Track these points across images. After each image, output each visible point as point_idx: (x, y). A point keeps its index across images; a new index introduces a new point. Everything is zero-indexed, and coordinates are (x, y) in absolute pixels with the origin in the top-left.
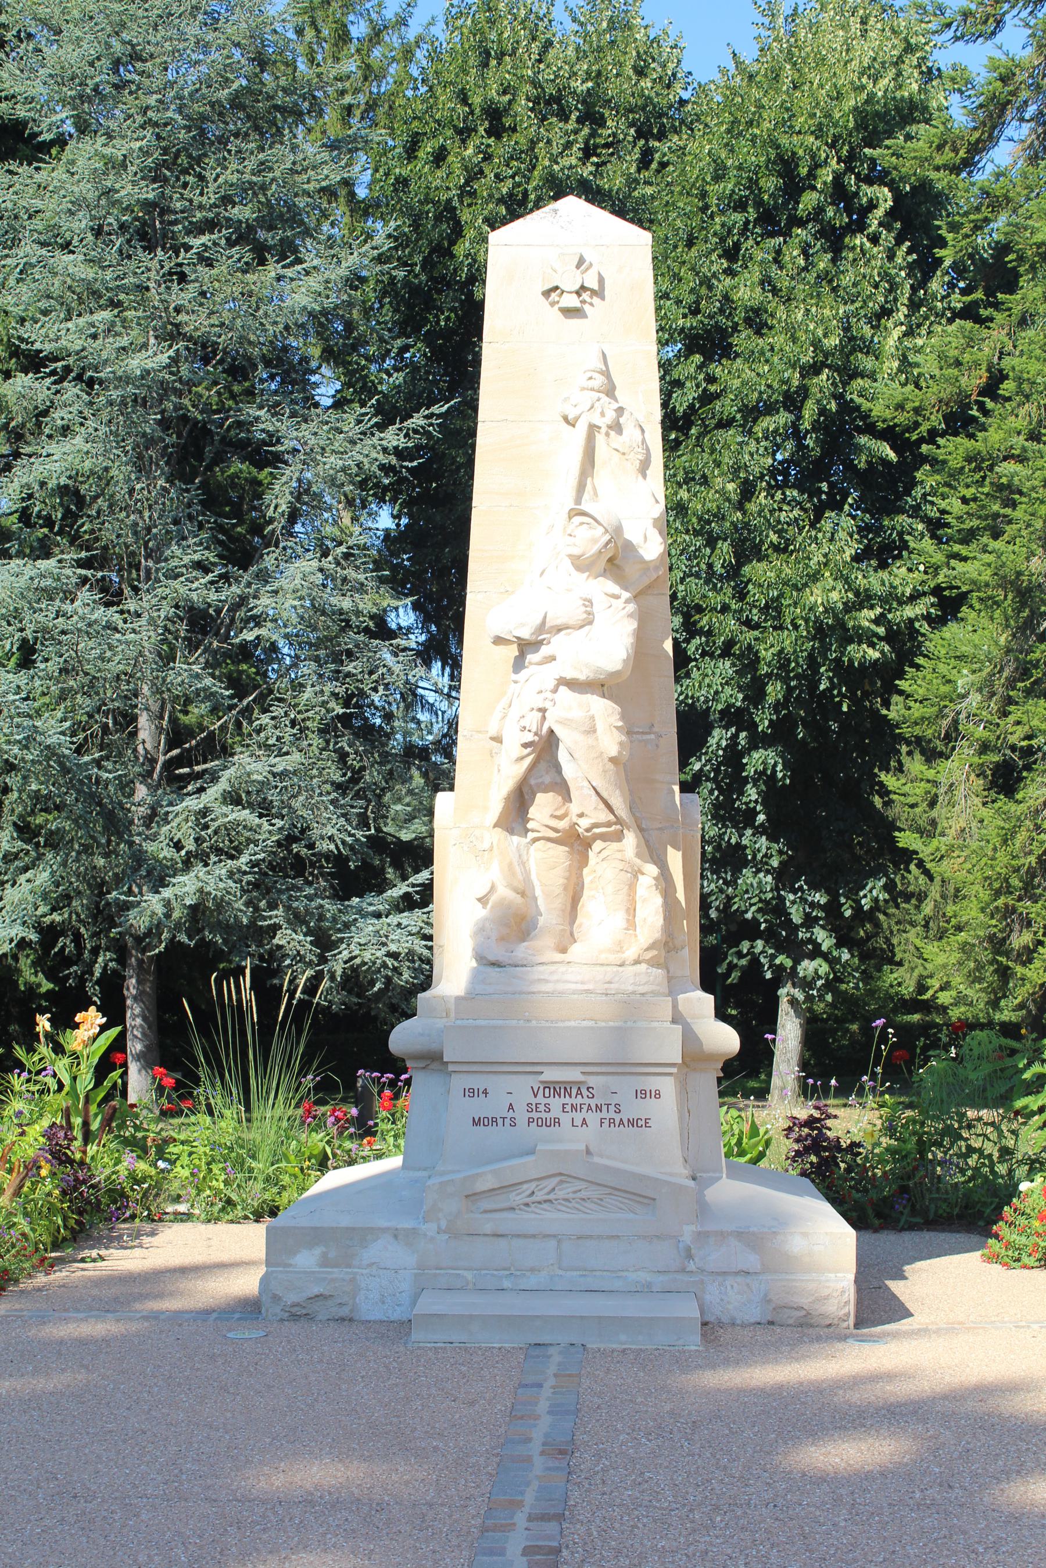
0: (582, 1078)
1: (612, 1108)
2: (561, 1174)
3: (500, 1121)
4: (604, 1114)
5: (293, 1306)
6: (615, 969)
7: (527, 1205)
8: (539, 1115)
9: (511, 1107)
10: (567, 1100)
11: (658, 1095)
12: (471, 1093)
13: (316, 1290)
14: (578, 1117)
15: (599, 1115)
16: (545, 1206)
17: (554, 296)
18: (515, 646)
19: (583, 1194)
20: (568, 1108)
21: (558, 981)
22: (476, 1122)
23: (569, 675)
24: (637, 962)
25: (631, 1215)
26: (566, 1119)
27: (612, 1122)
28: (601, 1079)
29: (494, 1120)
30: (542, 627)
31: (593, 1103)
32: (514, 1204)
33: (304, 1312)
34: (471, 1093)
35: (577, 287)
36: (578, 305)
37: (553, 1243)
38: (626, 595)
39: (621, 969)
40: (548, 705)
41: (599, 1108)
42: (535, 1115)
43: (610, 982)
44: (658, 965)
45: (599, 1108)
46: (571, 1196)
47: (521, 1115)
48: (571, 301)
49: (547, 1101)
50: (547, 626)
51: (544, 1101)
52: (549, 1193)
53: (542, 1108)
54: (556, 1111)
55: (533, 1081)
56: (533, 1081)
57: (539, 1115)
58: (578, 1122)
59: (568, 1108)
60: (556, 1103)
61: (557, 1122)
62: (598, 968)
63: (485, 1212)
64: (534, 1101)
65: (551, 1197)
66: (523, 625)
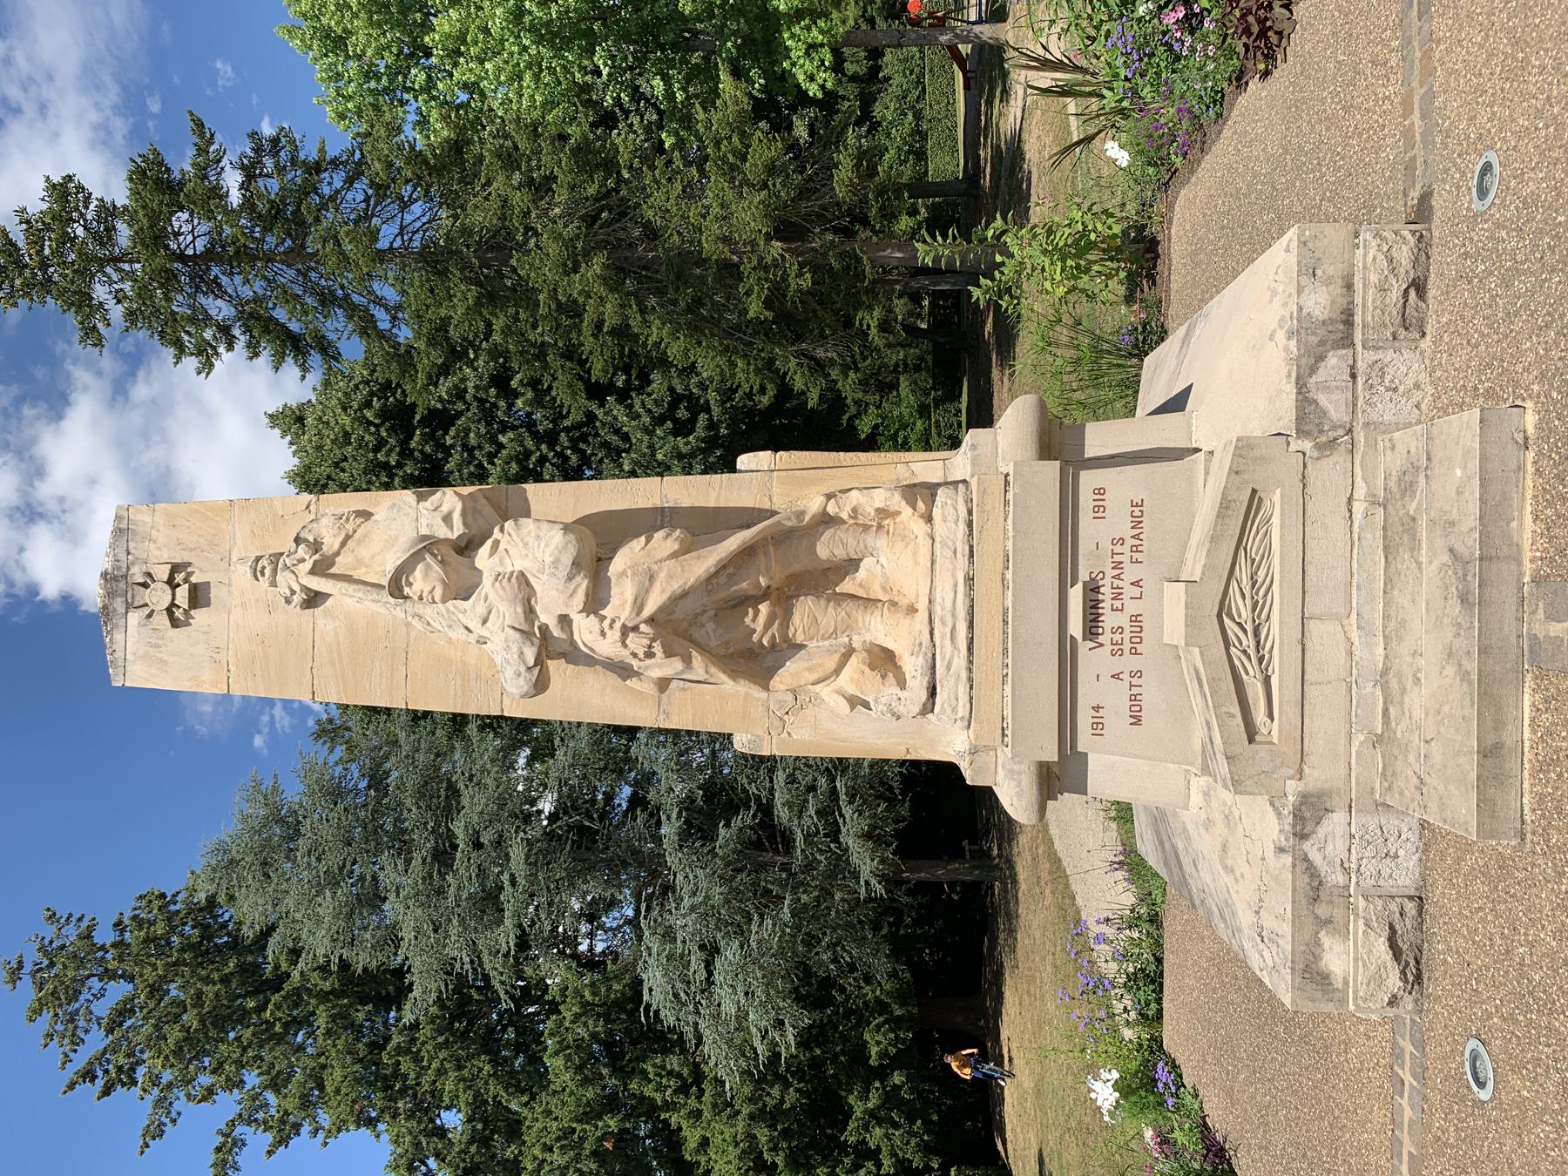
0: (1079, 587)
1: (1118, 549)
2: (1219, 616)
3: (1135, 690)
4: (1125, 559)
5: (1406, 981)
6: (938, 545)
7: (1261, 660)
8: (1126, 641)
11: (1100, 491)
12: (1097, 726)
13: (1382, 946)
15: (1127, 565)
17: (178, 614)
18: (552, 665)
20: (1117, 604)
21: (954, 616)
23: (579, 599)
24: (929, 519)
25: (1276, 520)
26: (1132, 608)
27: (1135, 549)
29: (1134, 698)
30: (526, 634)
31: (1110, 573)
33: (1412, 963)
35: (167, 588)
37: (1312, 626)
38: (496, 533)
39: (938, 539)
40: (618, 625)
41: (1118, 565)
42: (1127, 646)
43: (955, 552)
44: (934, 495)
45: (1118, 565)
47: (1128, 663)
48: (182, 594)
50: (525, 628)
52: (1245, 631)
53: (1117, 637)
54: (1122, 620)
55: (1084, 647)
57: (1126, 641)
58: (1136, 591)
59: (1117, 604)
60: (1109, 620)
61: (1135, 618)
62: (937, 566)
63: (1271, 716)
64: (1108, 647)
65: (1249, 628)
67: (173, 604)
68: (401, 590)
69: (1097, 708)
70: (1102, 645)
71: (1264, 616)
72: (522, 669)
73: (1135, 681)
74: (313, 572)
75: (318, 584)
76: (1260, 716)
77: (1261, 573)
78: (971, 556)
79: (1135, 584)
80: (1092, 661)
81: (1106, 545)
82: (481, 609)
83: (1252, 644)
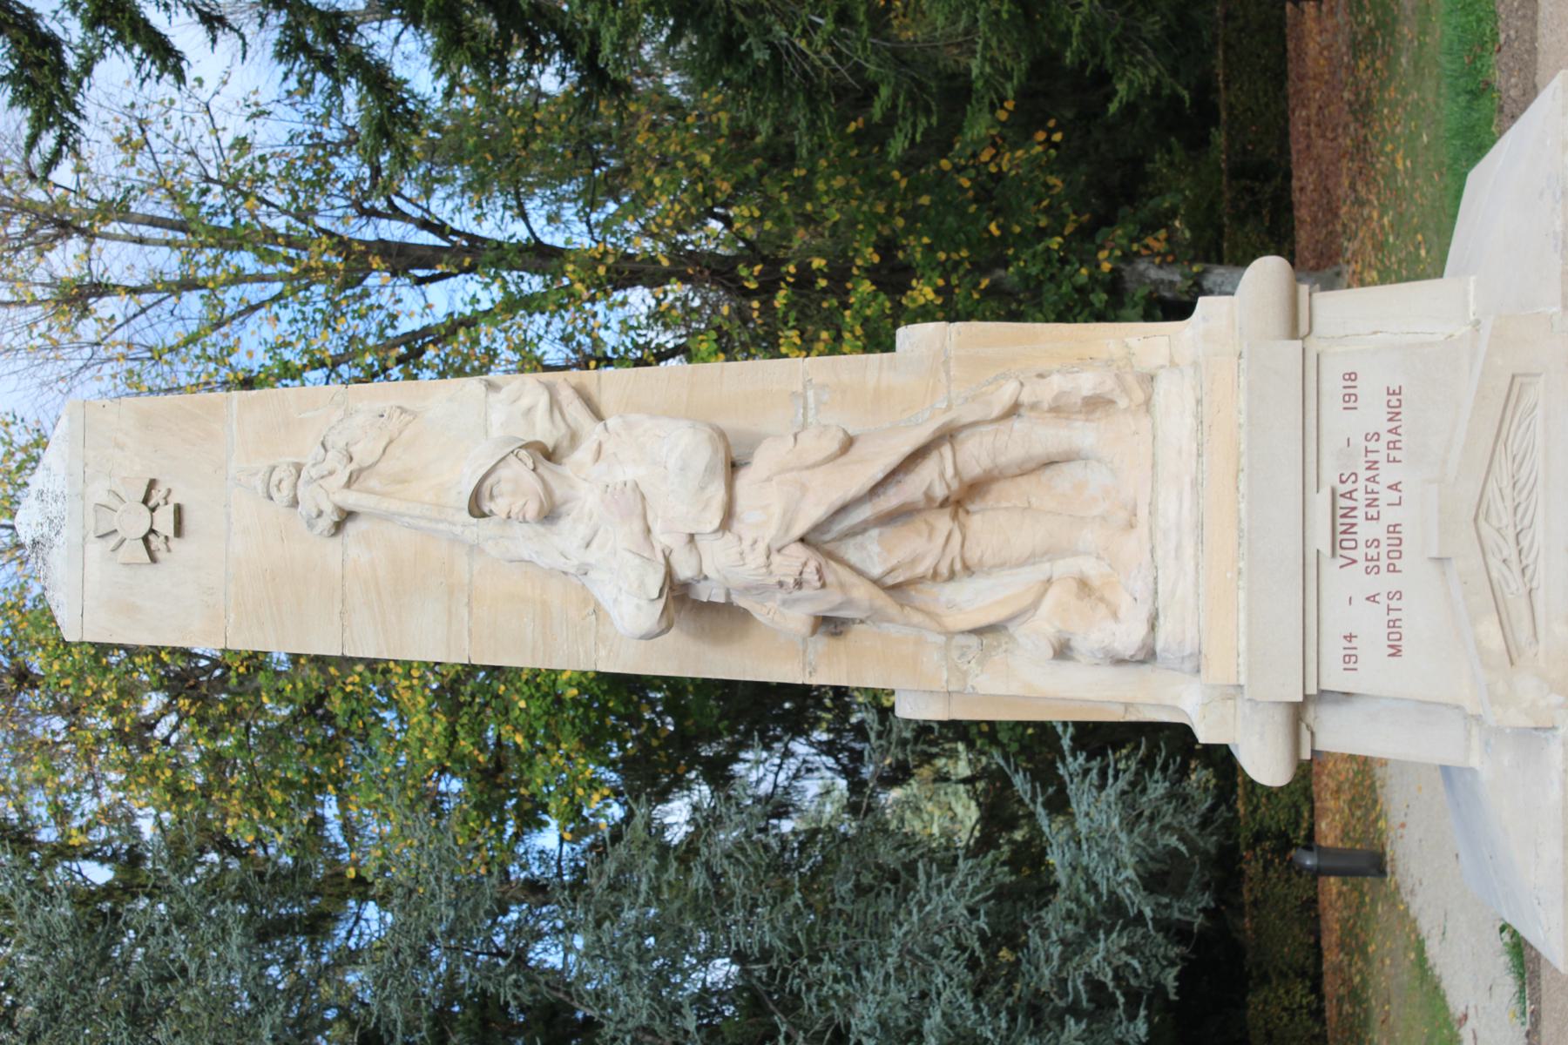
1: (1372, 445)
3: (1394, 615)
8: (1383, 556)
9: (1372, 599)
10: (1360, 513)
12: (1350, 659)
14: (1386, 496)
15: (1383, 464)
16: (1525, 543)
19: (1506, 483)
20: (1372, 512)
22: (1396, 651)
25: (1539, 412)
26: (1389, 516)
27: (1393, 446)
28: (1327, 462)
29: (1392, 624)
31: (1364, 474)
32: (1523, 591)
34: (1350, 659)
36: (171, 507)
40: (761, 547)
43: (1180, 452)
46: (1509, 503)
47: (1384, 582)
49: (1362, 544)
51: (1362, 548)
53: (1372, 552)
54: (1378, 530)
55: (1331, 568)
56: (1331, 568)
57: (1383, 556)
59: (1372, 512)
60: (1365, 531)
61: (1394, 529)
64: (1362, 564)
66: (642, 584)
67: (152, 531)
68: (479, 507)
69: (1349, 638)
70: (1354, 561)
71: (1527, 521)
72: (644, 603)
73: (1394, 604)
74: (349, 484)
75: (351, 500)
76: (1523, 633)
77: (1524, 471)
78: (1154, 466)
79: (1394, 487)
80: (1344, 585)
81: (1359, 442)
82: (583, 530)
83: (1514, 557)
